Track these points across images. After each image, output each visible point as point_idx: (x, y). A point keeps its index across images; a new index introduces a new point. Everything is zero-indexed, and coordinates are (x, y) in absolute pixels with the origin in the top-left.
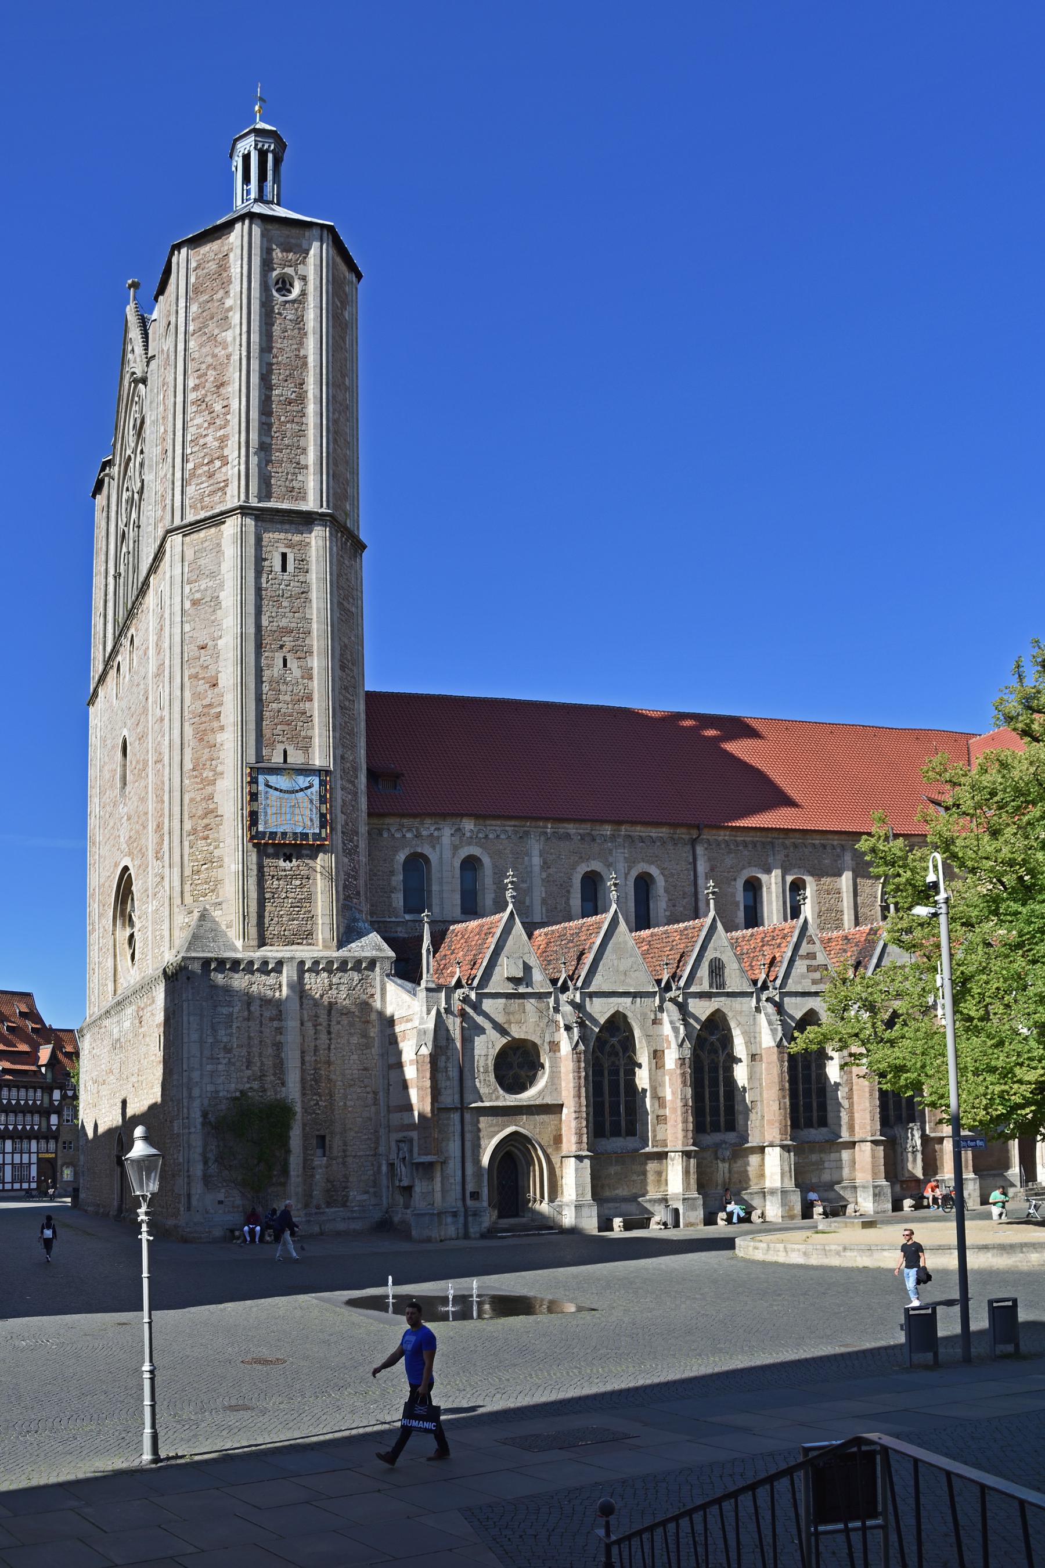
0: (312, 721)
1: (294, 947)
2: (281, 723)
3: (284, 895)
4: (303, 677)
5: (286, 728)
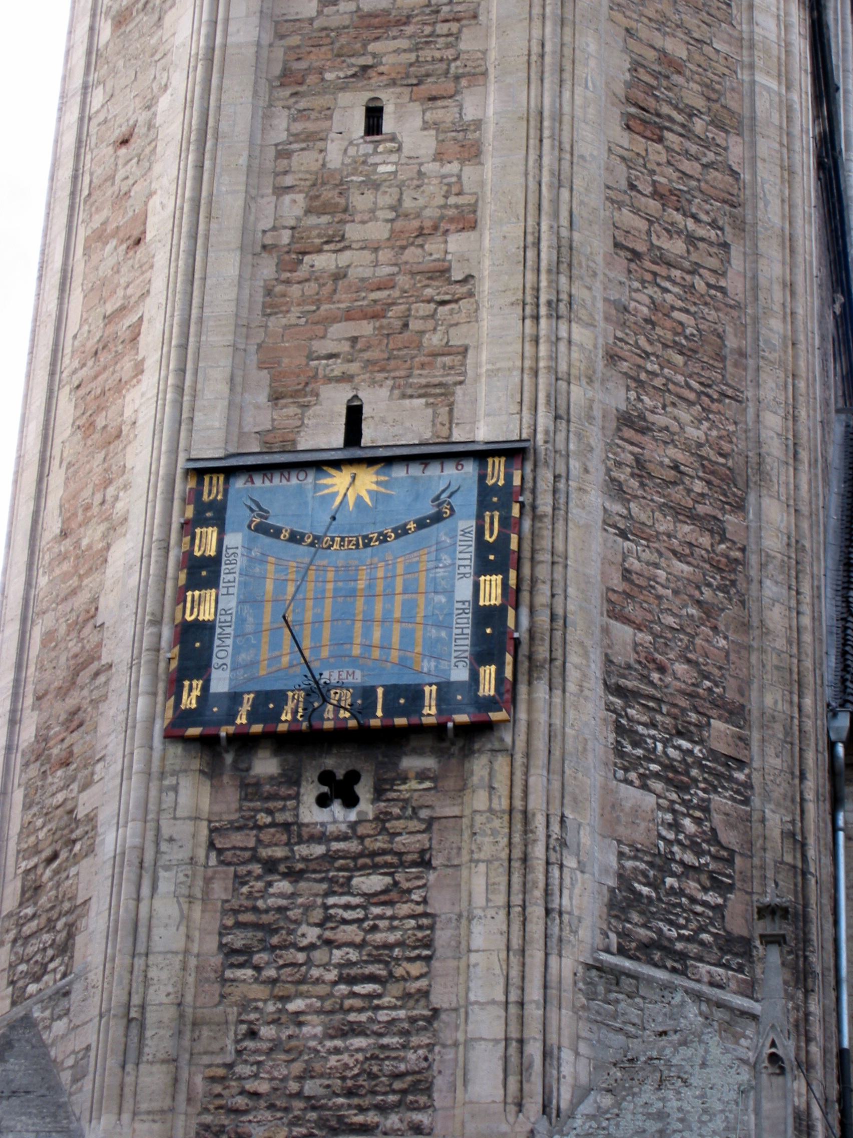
0: (471, 294)
2: (349, 315)
3: (312, 934)
4: (439, 157)
5: (366, 328)
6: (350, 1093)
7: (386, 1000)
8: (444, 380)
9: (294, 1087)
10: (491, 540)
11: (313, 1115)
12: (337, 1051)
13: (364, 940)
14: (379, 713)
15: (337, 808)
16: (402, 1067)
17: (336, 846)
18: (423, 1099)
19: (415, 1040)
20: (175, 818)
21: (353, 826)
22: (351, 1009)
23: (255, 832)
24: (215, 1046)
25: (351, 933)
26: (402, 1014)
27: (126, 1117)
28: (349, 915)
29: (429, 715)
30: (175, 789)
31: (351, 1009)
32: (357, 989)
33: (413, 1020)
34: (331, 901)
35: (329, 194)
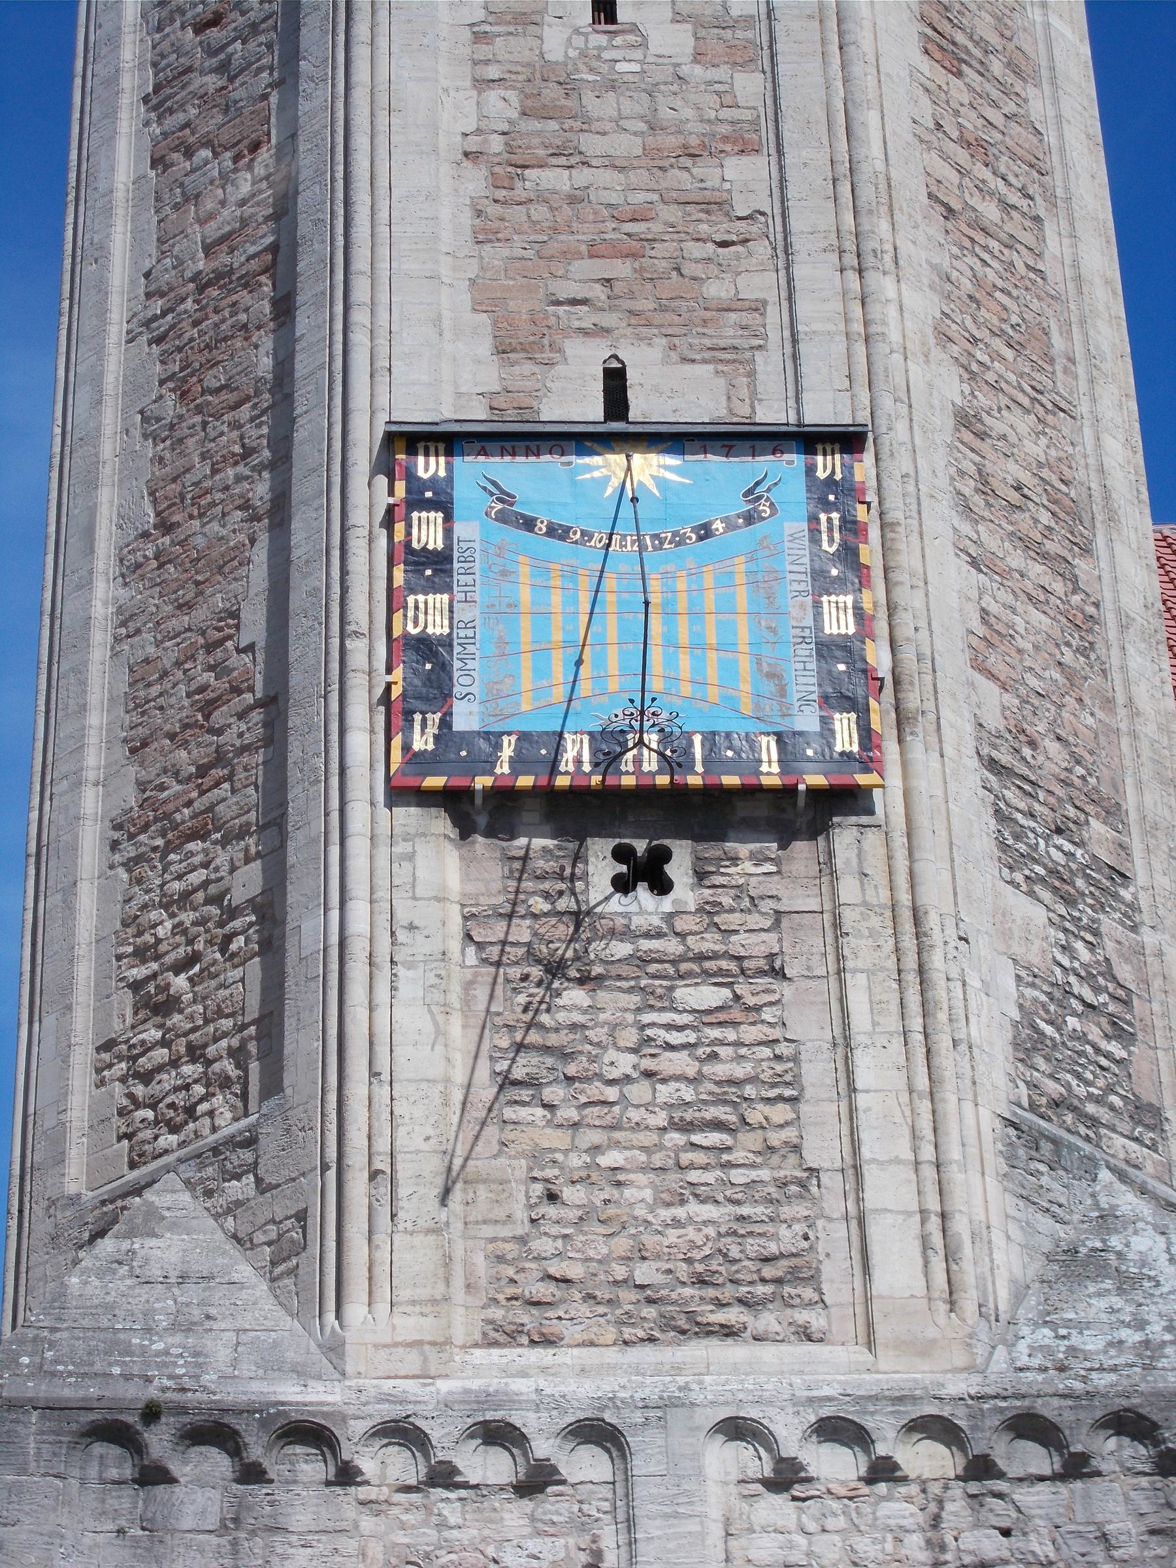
1: (696, 1351)
3: (625, 1063)
4: (698, 57)
5: (621, 269)
6: (701, 1281)
7: (738, 1156)
8: (736, 342)
9: (620, 1272)
10: (832, 550)
11: (650, 1312)
12: (677, 1223)
13: (700, 1072)
14: (699, 768)
15: (643, 892)
16: (773, 1248)
17: (646, 944)
18: (808, 1293)
19: (786, 1211)
20: (415, 898)
21: (669, 917)
22: (691, 1166)
23: (528, 922)
24: (499, 1213)
25: (680, 1062)
26: (764, 1174)
27: (382, 1308)
28: (675, 1038)
29: (769, 774)
30: (411, 857)
31: (691, 1166)
32: (697, 1138)
33: (783, 1184)
34: (647, 1018)
35: (552, 92)
